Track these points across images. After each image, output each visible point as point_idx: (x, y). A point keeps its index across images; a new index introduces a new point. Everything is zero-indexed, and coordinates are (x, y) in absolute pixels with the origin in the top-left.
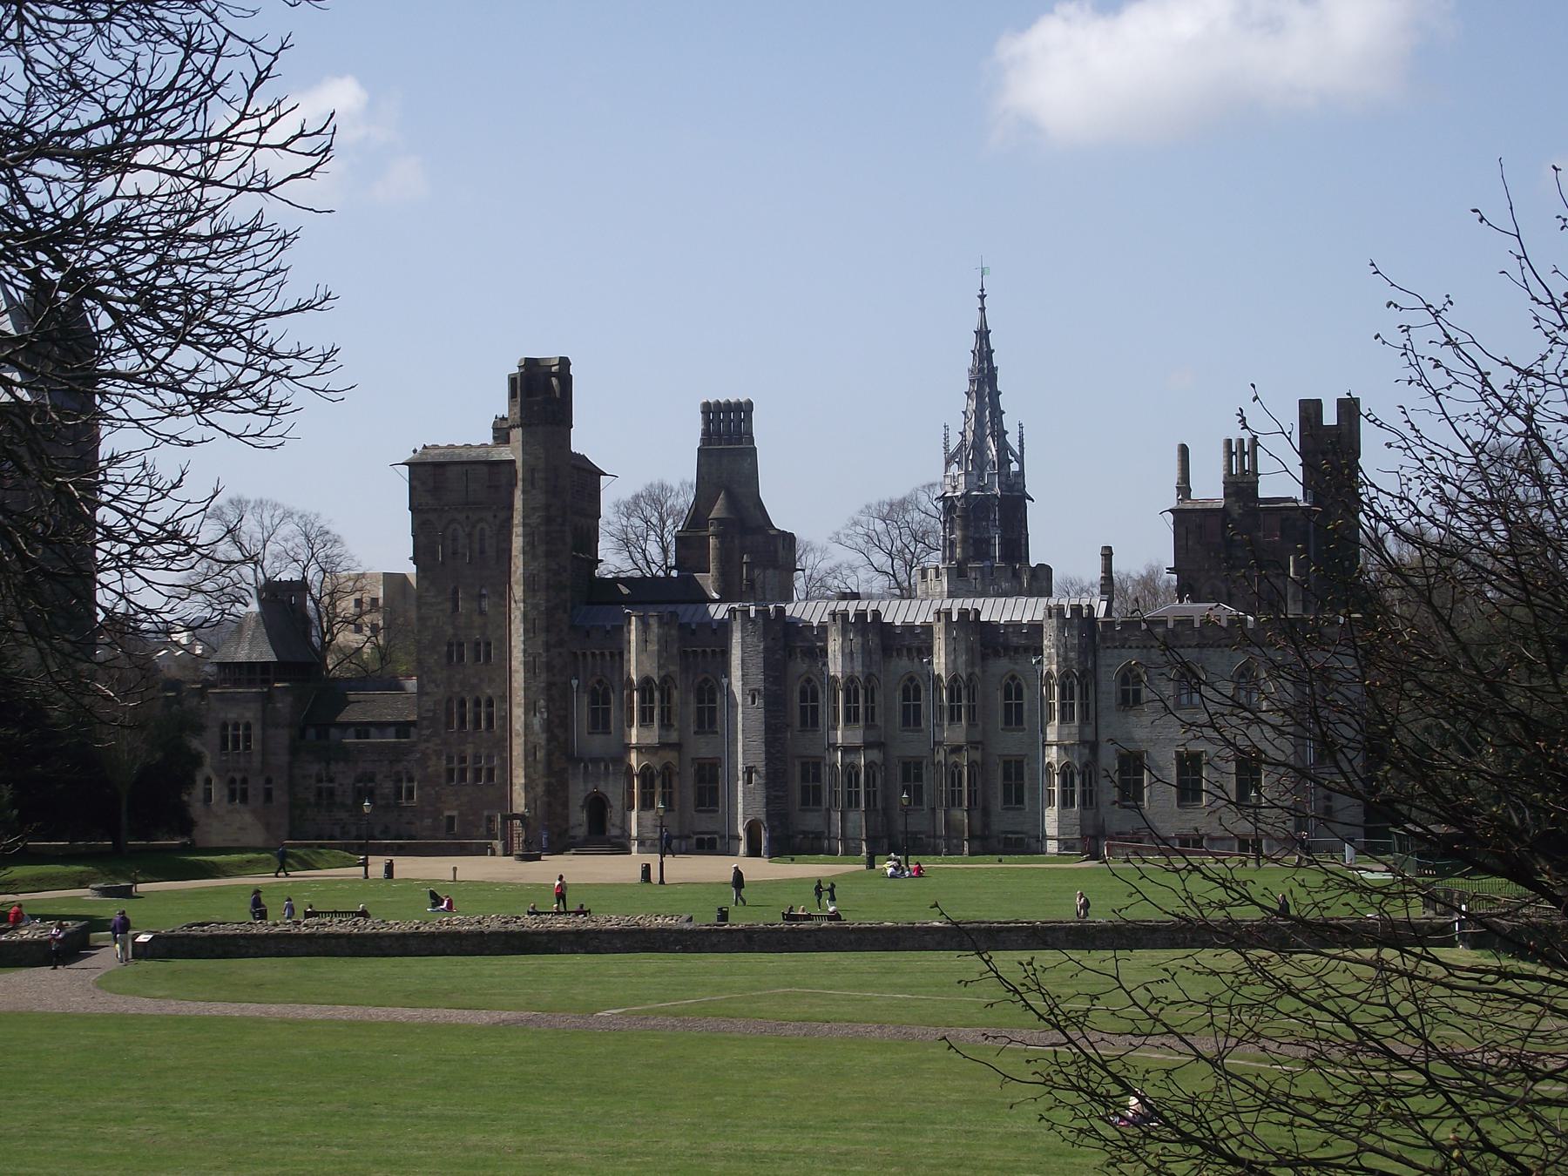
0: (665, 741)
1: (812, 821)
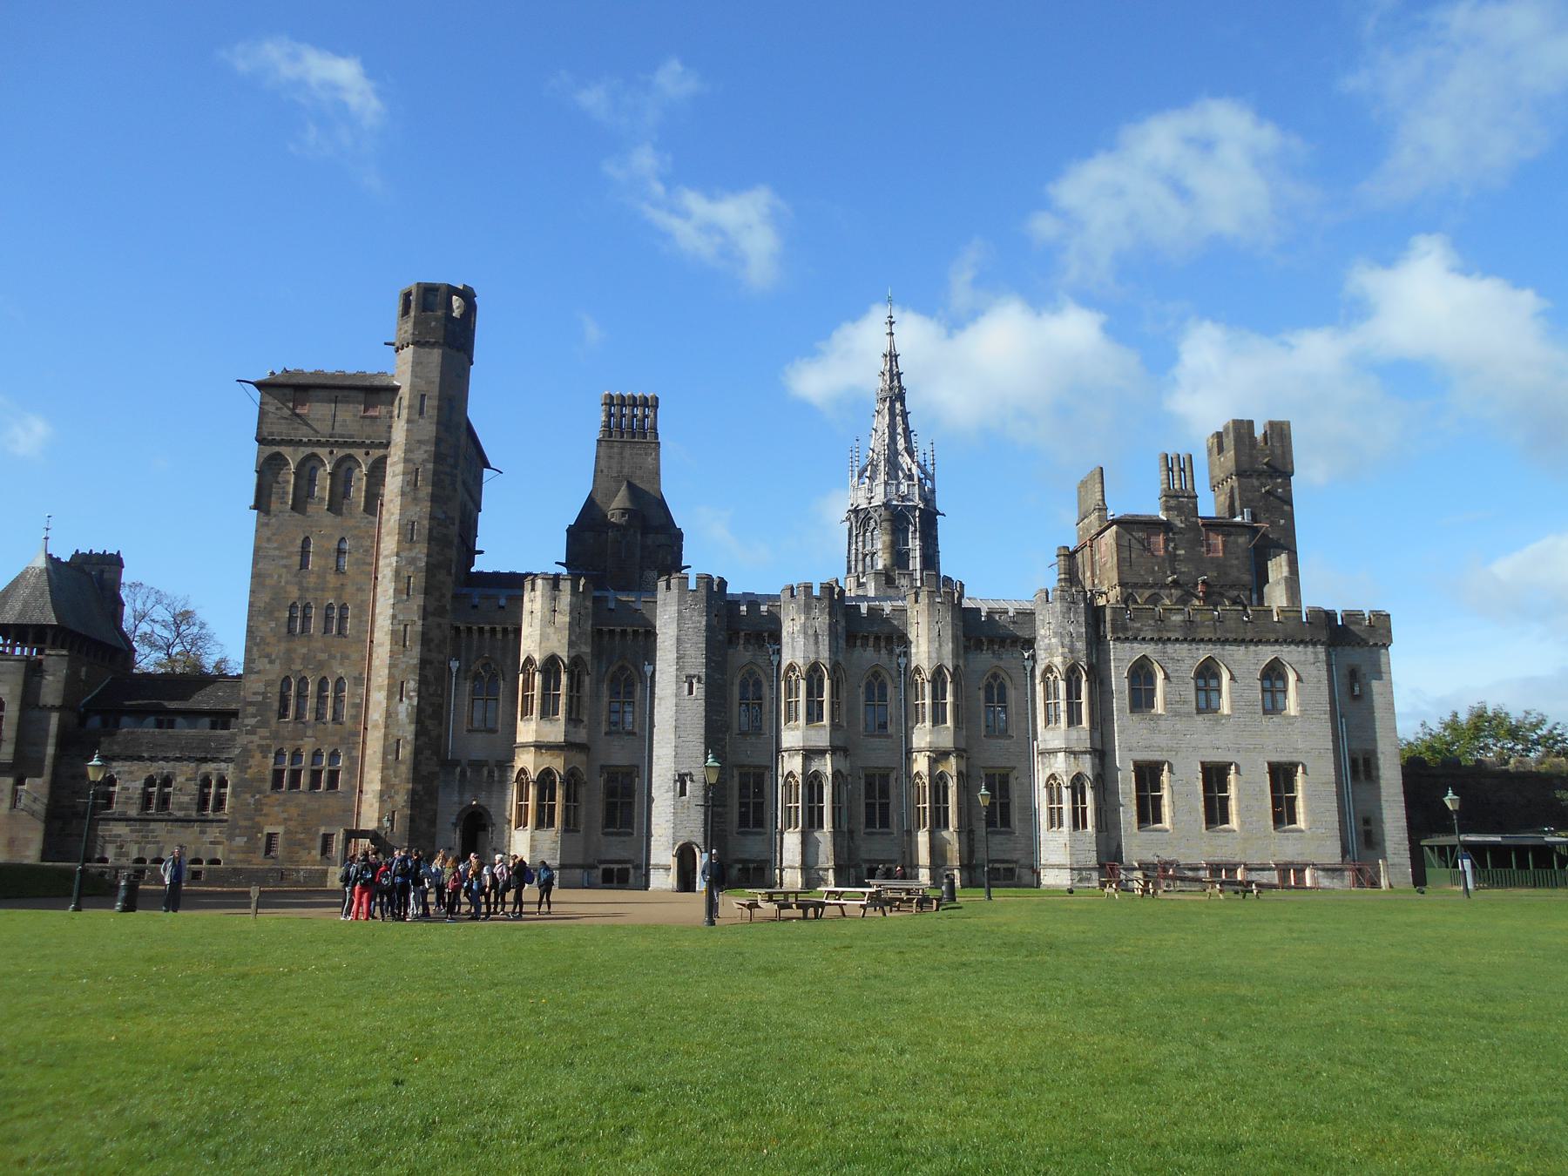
0: (573, 741)
1: (752, 847)
